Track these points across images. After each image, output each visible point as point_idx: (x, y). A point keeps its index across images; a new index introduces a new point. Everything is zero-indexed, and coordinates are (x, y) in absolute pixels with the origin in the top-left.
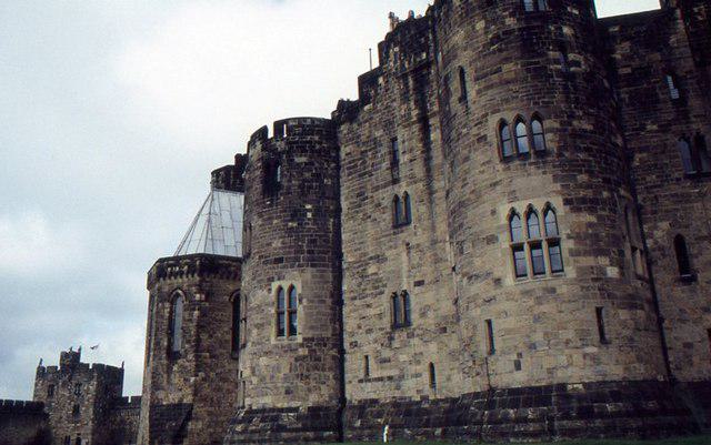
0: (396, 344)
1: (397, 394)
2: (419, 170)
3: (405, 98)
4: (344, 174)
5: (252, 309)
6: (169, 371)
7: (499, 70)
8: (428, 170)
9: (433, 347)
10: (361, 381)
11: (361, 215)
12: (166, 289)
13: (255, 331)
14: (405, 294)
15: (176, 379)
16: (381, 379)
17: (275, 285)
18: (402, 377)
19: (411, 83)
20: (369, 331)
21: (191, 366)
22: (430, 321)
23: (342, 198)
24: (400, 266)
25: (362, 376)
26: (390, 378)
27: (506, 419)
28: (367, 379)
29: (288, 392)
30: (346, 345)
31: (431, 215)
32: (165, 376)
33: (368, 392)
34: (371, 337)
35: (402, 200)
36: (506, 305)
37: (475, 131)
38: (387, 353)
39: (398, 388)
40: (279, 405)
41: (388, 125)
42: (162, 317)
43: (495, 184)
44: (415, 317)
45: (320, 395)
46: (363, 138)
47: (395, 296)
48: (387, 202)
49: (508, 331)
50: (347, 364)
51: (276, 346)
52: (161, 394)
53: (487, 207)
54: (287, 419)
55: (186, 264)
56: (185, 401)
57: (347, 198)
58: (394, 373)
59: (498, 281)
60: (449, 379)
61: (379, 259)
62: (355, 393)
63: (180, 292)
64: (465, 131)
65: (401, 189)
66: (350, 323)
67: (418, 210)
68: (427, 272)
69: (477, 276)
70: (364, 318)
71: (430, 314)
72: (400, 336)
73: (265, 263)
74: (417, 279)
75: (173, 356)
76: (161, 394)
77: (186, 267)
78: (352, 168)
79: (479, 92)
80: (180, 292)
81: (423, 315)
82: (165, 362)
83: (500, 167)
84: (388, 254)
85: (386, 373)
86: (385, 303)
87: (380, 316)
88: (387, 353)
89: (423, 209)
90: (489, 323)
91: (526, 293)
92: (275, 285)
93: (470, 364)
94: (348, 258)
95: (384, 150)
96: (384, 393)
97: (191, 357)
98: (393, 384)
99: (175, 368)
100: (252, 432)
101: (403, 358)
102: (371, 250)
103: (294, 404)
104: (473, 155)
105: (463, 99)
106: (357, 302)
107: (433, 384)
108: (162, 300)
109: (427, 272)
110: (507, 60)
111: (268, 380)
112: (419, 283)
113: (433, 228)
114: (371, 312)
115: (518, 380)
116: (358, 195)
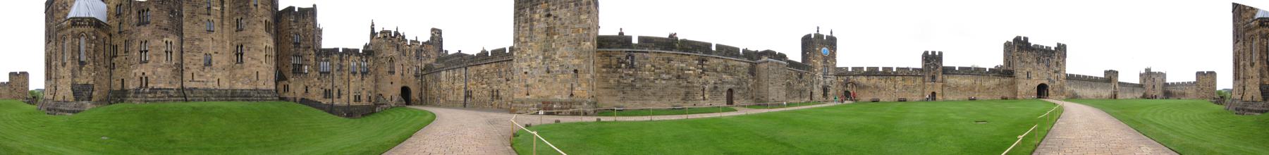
2: (219, 15)
6: (81, 69)
15: (84, 73)
33: (193, 85)
44: (214, 63)
45: (178, 86)
54: (172, 93)
61: (200, 40)
62: (187, 85)
65: (211, 18)
66: (186, 60)
67: (217, 28)
68: (219, 50)
70: (193, 63)
72: (207, 68)
86: (202, 56)
94: (185, 36)
102: (197, 36)
109: (219, 50)
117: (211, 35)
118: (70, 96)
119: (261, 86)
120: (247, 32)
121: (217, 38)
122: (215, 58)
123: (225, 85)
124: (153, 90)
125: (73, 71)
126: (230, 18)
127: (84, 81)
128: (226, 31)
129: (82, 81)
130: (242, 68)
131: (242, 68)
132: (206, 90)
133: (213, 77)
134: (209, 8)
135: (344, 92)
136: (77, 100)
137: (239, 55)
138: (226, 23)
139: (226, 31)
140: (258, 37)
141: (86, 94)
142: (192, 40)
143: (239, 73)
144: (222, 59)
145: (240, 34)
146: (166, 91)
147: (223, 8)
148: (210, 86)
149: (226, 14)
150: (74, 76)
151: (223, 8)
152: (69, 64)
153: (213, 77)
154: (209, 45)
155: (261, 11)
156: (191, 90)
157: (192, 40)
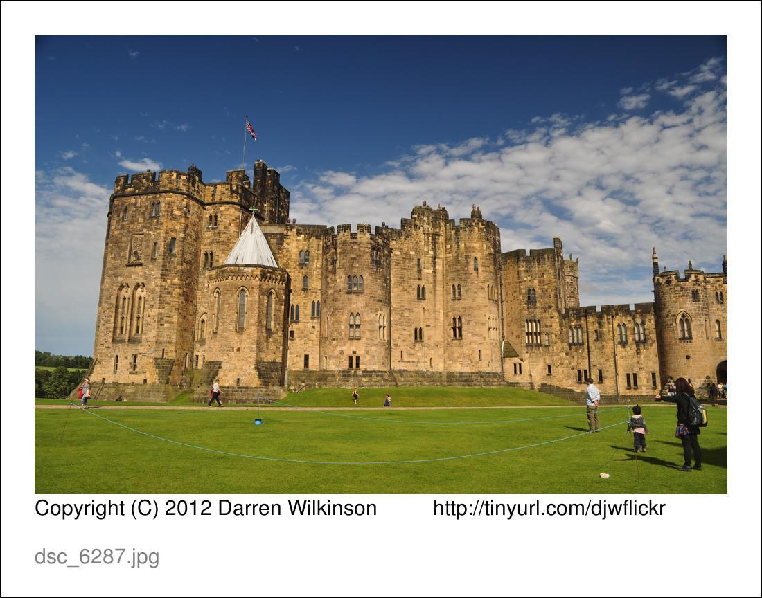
0: (417, 348)
1: (416, 368)
2: (431, 279)
3: (426, 244)
4: (393, 264)
5: (365, 321)
6: (268, 339)
7: (489, 267)
8: (435, 280)
9: (432, 352)
10: (399, 361)
11: (402, 287)
12: (265, 287)
13: (368, 334)
14: (421, 329)
16: (409, 362)
17: (379, 313)
18: (418, 362)
19: (430, 238)
20: (404, 341)
21: (281, 340)
22: (432, 342)
23: (392, 276)
24: (419, 314)
25: (400, 359)
26: (413, 362)
27: (489, 381)
28: (402, 361)
29: (383, 364)
30: (392, 345)
31: (435, 300)
32: (265, 344)
33: (402, 366)
34: (405, 343)
35: (213, 217)
36: (486, 346)
37: (481, 284)
38: (412, 351)
39: (417, 366)
40: (380, 370)
41: (417, 251)
42: (263, 305)
43: (486, 306)
44: (425, 338)
46: (405, 251)
47: (416, 329)
48: (415, 287)
49: (487, 355)
50: (392, 353)
51: (379, 342)
52: (263, 355)
53: (482, 313)
55: (280, 274)
56: (277, 361)
57: (394, 277)
58: (416, 360)
59: (484, 338)
60: (438, 365)
61: (410, 310)
62: (396, 366)
63: (273, 290)
64: (476, 282)
65: (422, 283)
66: (395, 335)
67: (427, 295)
68: (431, 322)
69: (477, 335)
70: (402, 336)
71: (432, 339)
72: (418, 345)
73: (374, 300)
74: (428, 324)
75: (268, 330)
76: (263, 355)
77: (279, 277)
78: (398, 263)
79: (483, 271)
80: (273, 290)
81: (429, 339)
82: (265, 335)
83: (488, 301)
84: (414, 309)
85: (411, 360)
87: (410, 335)
88: (412, 351)
89: (431, 296)
90: (480, 351)
91: (492, 344)
92: (379, 313)
93: (470, 362)
94: (394, 305)
95: (415, 262)
96: (411, 367)
97: (280, 334)
98: (414, 364)
99: (271, 340)
100: (375, 381)
101: (419, 354)
103: (385, 370)
104: (479, 293)
105: (476, 269)
106: (398, 326)
107: (431, 367)
108: (263, 294)
110: (491, 264)
111: (376, 358)
112: (428, 326)
113: (435, 306)
114: (406, 332)
115: (488, 370)
116: (401, 278)
117: (423, 304)
118: (250, 377)
119: (485, 368)
120: (466, 301)
121: (429, 307)
122: (426, 333)
123: (440, 367)
124: (367, 373)
125: (258, 343)
126: (445, 282)
127: (270, 358)
128: (440, 298)
129: (268, 358)
130: (460, 346)
131: (460, 346)
132: (417, 372)
133: (425, 356)
134: (419, 271)
135: (609, 374)
136: (266, 384)
137: (458, 331)
138: (439, 288)
139: (440, 298)
140: (479, 308)
141: (275, 375)
142: (401, 310)
143: (457, 352)
144: (437, 332)
145: (457, 304)
146: (379, 374)
147: (435, 271)
148: (422, 367)
149: (439, 277)
150: (259, 349)
151: (435, 271)
152: (252, 331)
153: (425, 356)
154: (419, 314)
155: (482, 277)
156: (401, 372)
157: (401, 310)
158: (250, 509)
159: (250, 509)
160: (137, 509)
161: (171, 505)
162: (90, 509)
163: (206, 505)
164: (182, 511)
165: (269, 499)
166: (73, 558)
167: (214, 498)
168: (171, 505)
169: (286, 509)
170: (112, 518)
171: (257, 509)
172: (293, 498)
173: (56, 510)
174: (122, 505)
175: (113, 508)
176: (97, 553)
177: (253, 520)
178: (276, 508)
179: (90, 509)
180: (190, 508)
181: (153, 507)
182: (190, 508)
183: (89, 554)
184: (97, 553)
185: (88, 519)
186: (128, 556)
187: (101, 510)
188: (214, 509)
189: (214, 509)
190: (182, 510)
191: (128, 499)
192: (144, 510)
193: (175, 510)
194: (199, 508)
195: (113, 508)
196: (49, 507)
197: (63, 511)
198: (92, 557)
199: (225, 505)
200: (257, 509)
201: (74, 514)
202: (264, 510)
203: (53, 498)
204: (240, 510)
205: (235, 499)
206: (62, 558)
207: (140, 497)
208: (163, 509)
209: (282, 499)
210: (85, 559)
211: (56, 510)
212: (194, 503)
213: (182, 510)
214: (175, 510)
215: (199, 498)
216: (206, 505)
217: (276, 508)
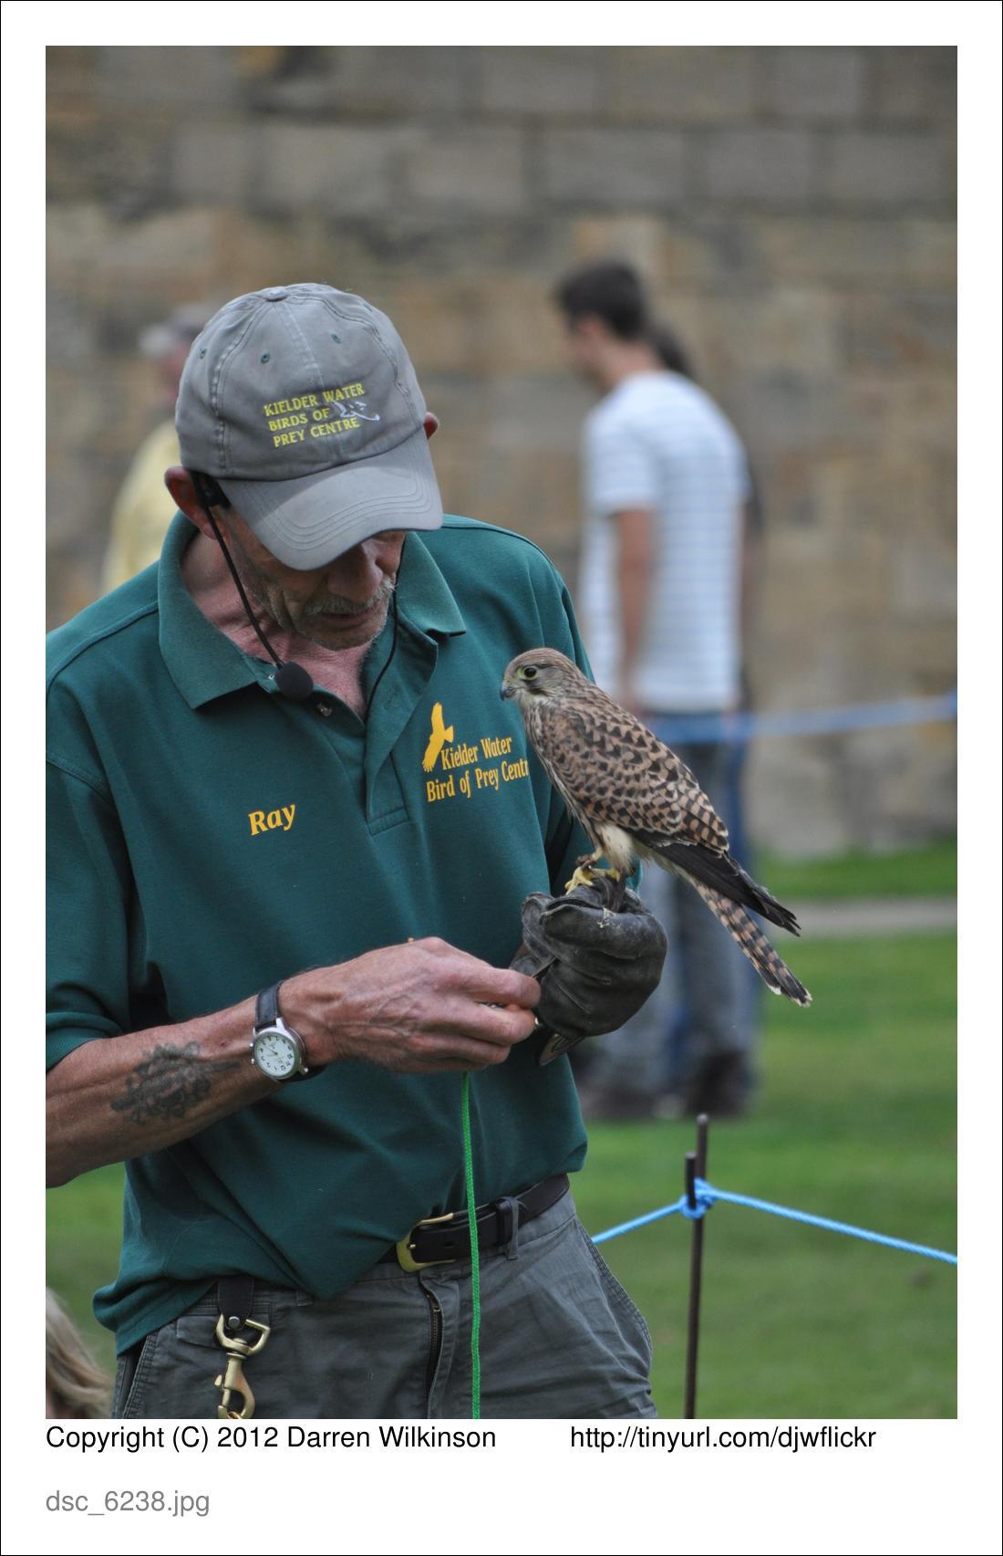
158: (330, 1438)
159: (330, 1438)
160: (181, 1439)
161: (225, 1433)
162: (118, 1438)
163: (272, 1433)
164: (240, 1441)
165: (354, 1425)
166: (96, 1503)
167: (282, 1425)
168: (225, 1433)
169: (376, 1439)
170: (147, 1451)
171: (338, 1438)
172: (386, 1423)
173: (73, 1439)
174: (160, 1433)
175: (149, 1437)
176: (127, 1497)
177: (333, 1454)
178: (363, 1437)
179: (118, 1438)
180: (251, 1437)
181: (201, 1436)
182: (251, 1437)
183: (118, 1498)
184: (127, 1497)
185: (116, 1452)
186: (169, 1502)
187: (133, 1440)
188: (282, 1439)
189: (282, 1439)
190: (240, 1440)
191: (169, 1425)
192: (190, 1441)
193: (230, 1440)
194: (262, 1438)
195: (149, 1437)
196: (64, 1436)
197: (83, 1442)
198: (121, 1501)
199: (296, 1433)
200: (338, 1438)
201: (98, 1445)
202: (347, 1439)
203: (71, 1425)
204: (316, 1441)
205: (310, 1425)
206: (82, 1503)
207: (184, 1423)
208: (214, 1438)
209: (371, 1425)
210: (111, 1505)
211: (73, 1439)
212: (255, 1431)
213: (240, 1440)
214: (230, 1440)
215: (262, 1424)
216: (272, 1433)
217: (363, 1437)
